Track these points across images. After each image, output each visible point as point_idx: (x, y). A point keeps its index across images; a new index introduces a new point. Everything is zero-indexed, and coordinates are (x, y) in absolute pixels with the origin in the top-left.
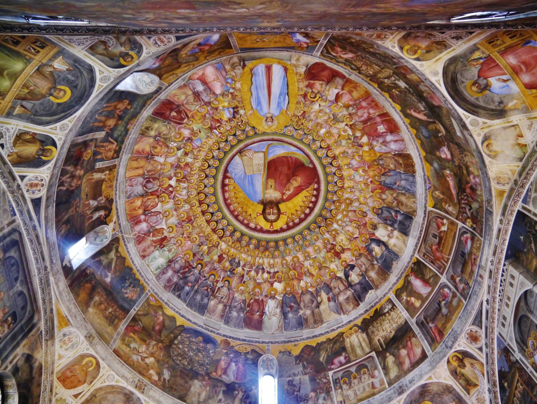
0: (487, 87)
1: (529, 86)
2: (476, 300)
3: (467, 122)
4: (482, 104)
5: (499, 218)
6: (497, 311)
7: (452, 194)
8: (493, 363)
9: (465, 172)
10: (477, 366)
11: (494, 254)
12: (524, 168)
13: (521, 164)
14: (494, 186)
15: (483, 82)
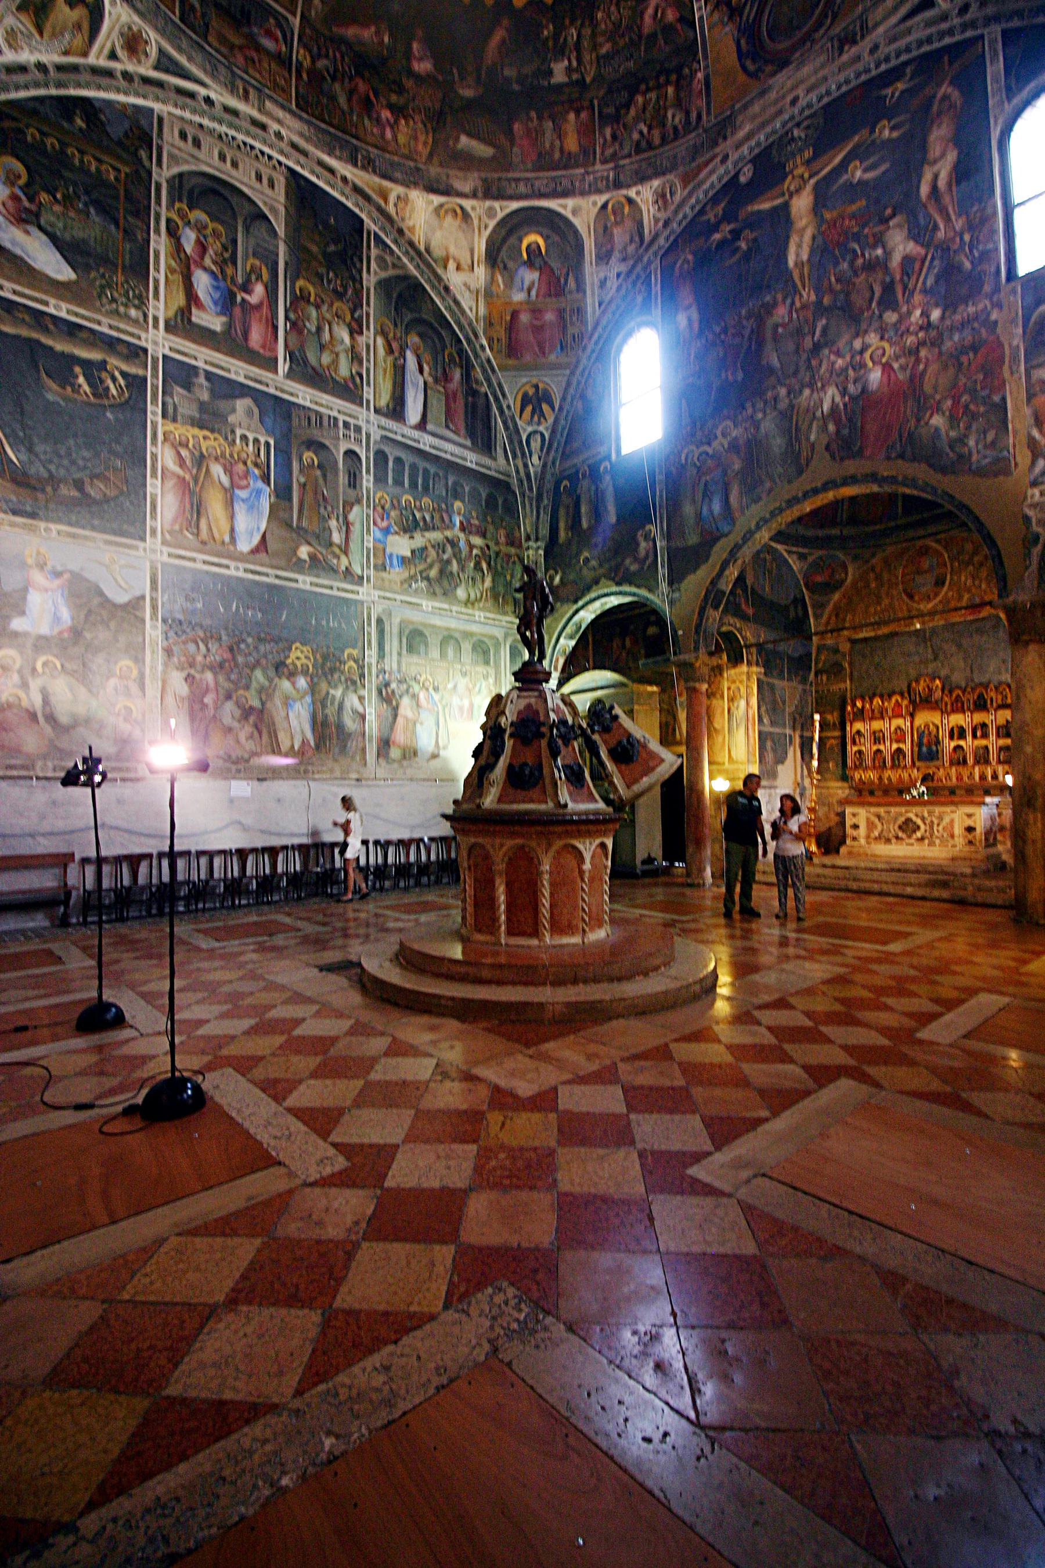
0: (530, 264)
1: (515, 314)
2: (205, 71)
3: (497, 205)
4: (512, 240)
5: (349, 176)
6: (197, 119)
7: (348, 25)
8: (99, 87)
9: (394, 98)
10: (79, 41)
11: (294, 146)
12: (419, 254)
13: (422, 248)
14: (396, 190)
15: (538, 262)
